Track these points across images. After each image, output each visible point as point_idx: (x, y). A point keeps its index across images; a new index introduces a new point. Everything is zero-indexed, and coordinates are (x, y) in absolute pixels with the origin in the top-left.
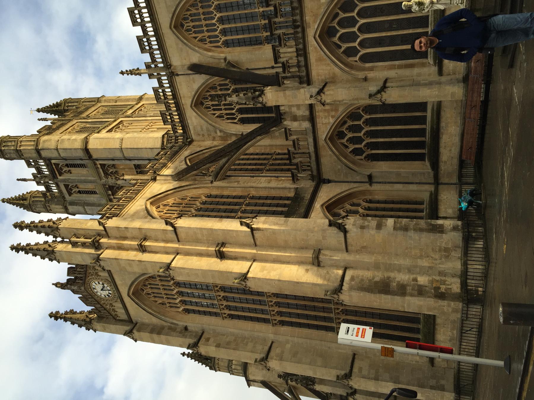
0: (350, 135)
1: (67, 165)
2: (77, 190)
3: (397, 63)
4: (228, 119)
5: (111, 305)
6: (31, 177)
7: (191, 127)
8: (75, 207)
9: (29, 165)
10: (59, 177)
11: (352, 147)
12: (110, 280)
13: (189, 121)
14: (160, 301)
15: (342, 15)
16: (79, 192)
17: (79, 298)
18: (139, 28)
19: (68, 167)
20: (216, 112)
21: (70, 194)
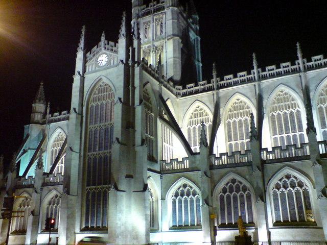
0: (185, 191)
1: (162, 23)
11: (180, 192)
16: (146, 28)
21: (144, 23)
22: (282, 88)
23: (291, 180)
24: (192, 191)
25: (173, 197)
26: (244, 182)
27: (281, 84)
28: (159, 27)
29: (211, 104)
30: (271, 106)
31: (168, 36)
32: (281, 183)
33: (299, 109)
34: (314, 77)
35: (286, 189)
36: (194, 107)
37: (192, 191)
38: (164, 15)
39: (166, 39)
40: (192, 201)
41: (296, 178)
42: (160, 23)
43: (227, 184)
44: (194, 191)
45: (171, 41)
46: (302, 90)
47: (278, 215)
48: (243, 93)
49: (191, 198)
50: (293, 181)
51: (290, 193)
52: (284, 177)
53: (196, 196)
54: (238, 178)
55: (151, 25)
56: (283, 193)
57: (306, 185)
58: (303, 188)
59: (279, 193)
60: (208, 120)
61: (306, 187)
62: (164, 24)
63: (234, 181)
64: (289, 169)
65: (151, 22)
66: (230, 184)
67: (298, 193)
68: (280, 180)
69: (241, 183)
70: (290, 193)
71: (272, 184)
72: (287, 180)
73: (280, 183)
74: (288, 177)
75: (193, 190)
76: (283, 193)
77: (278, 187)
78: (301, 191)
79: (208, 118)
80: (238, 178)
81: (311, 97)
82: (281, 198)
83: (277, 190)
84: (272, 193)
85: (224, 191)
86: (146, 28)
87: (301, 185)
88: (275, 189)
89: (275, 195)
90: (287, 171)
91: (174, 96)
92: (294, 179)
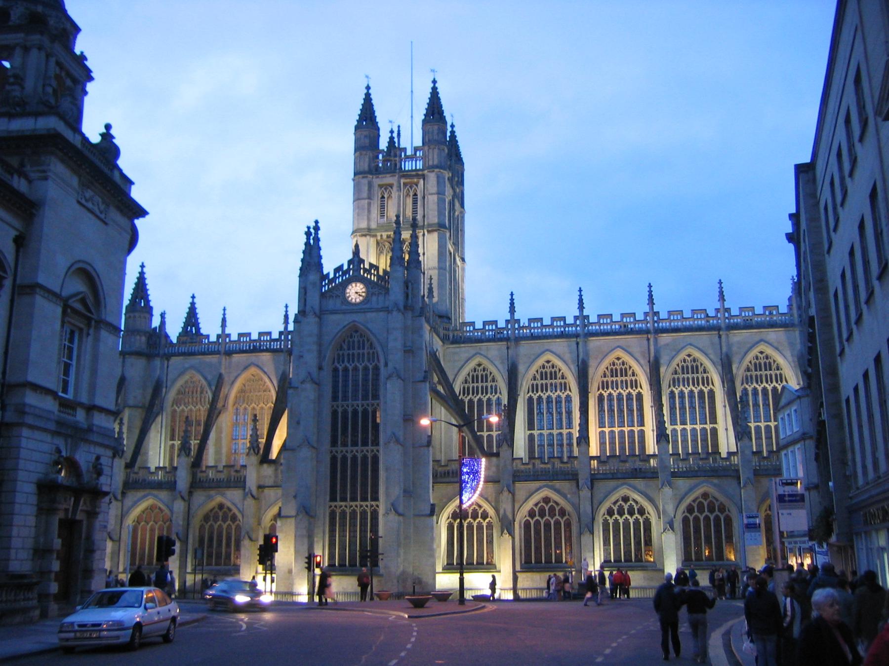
1: (415, 195)
2: (386, 196)
3: (523, 544)
4: (464, 388)
5: (337, 296)
6: (402, 146)
7: (458, 350)
8: (366, 188)
9: (416, 149)
10: (402, 181)
12: (368, 306)
13: (463, 349)
14: (345, 347)
15: (557, 509)
16: (383, 197)
17: (342, 266)
18: (549, 323)
19: (414, 196)
20: (471, 377)
21: (381, 186)
22: (619, 353)
23: (628, 504)
24: (480, 512)
25: (449, 520)
26: (562, 502)
27: (619, 347)
28: (409, 201)
29: (502, 363)
30: (600, 380)
31: (429, 225)
32: (615, 508)
33: (641, 391)
34: (667, 345)
35: (621, 516)
36: (472, 364)
37: (480, 512)
38: (422, 181)
39: (426, 231)
40: (480, 527)
41: (636, 502)
42: (411, 194)
43: (536, 505)
44: (484, 511)
45: (435, 235)
46: (649, 362)
47: (607, 552)
48: (558, 352)
49: (479, 523)
50: (631, 506)
51: (626, 523)
52: (620, 499)
53: (487, 520)
54: (555, 497)
55: (395, 194)
56: (616, 522)
57: (648, 513)
58: (644, 517)
59: (611, 521)
60: (496, 389)
61: (648, 515)
62: (419, 197)
63: (546, 500)
64: (628, 489)
65: (395, 188)
66: (542, 504)
67: (637, 522)
68: (615, 503)
69: (557, 504)
70: (626, 523)
71: (603, 509)
72: (623, 504)
73: (614, 508)
74: (626, 499)
75: (482, 510)
76: (616, 522)
77: (610, 512)
78: (641, 521)
79: (496, 386)
80: (555, 497)
81: (662, 375)
82: (613, 529)
83: (608, 518)
84: (601, 521)
85: (532, 514)
86: (383, 197)
87: (642, 511)
88: (606, 516)
89: (606, 524)
90: (624, 491)
91: (441, 343)
92: (633, 504)
